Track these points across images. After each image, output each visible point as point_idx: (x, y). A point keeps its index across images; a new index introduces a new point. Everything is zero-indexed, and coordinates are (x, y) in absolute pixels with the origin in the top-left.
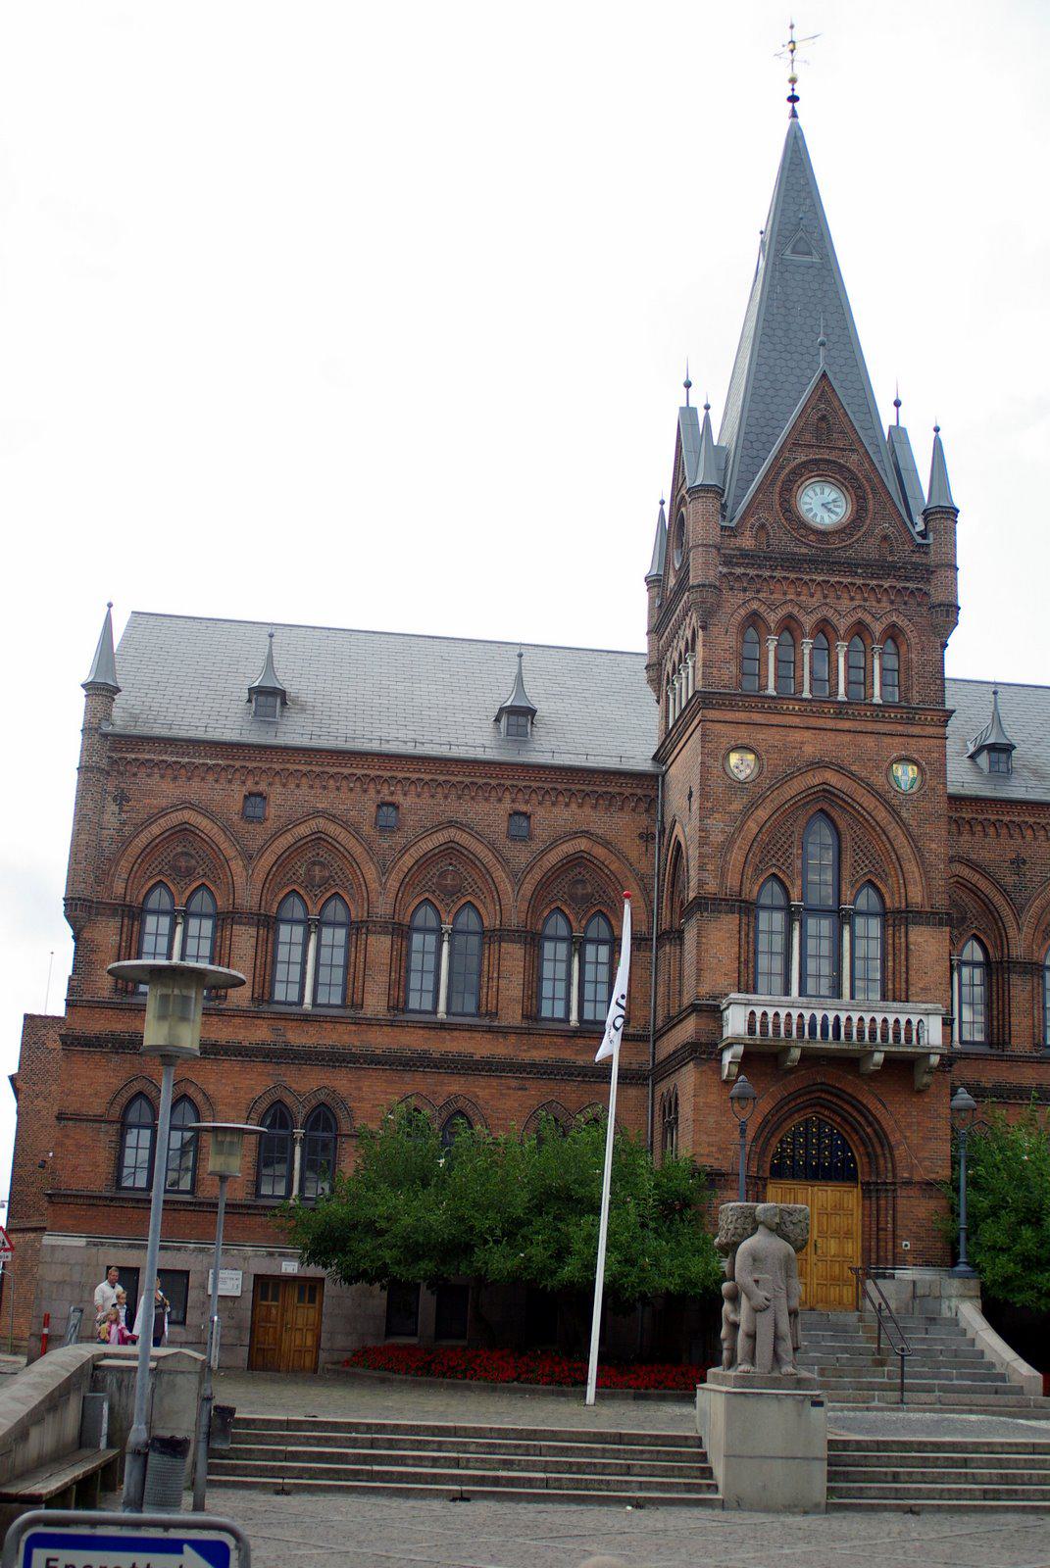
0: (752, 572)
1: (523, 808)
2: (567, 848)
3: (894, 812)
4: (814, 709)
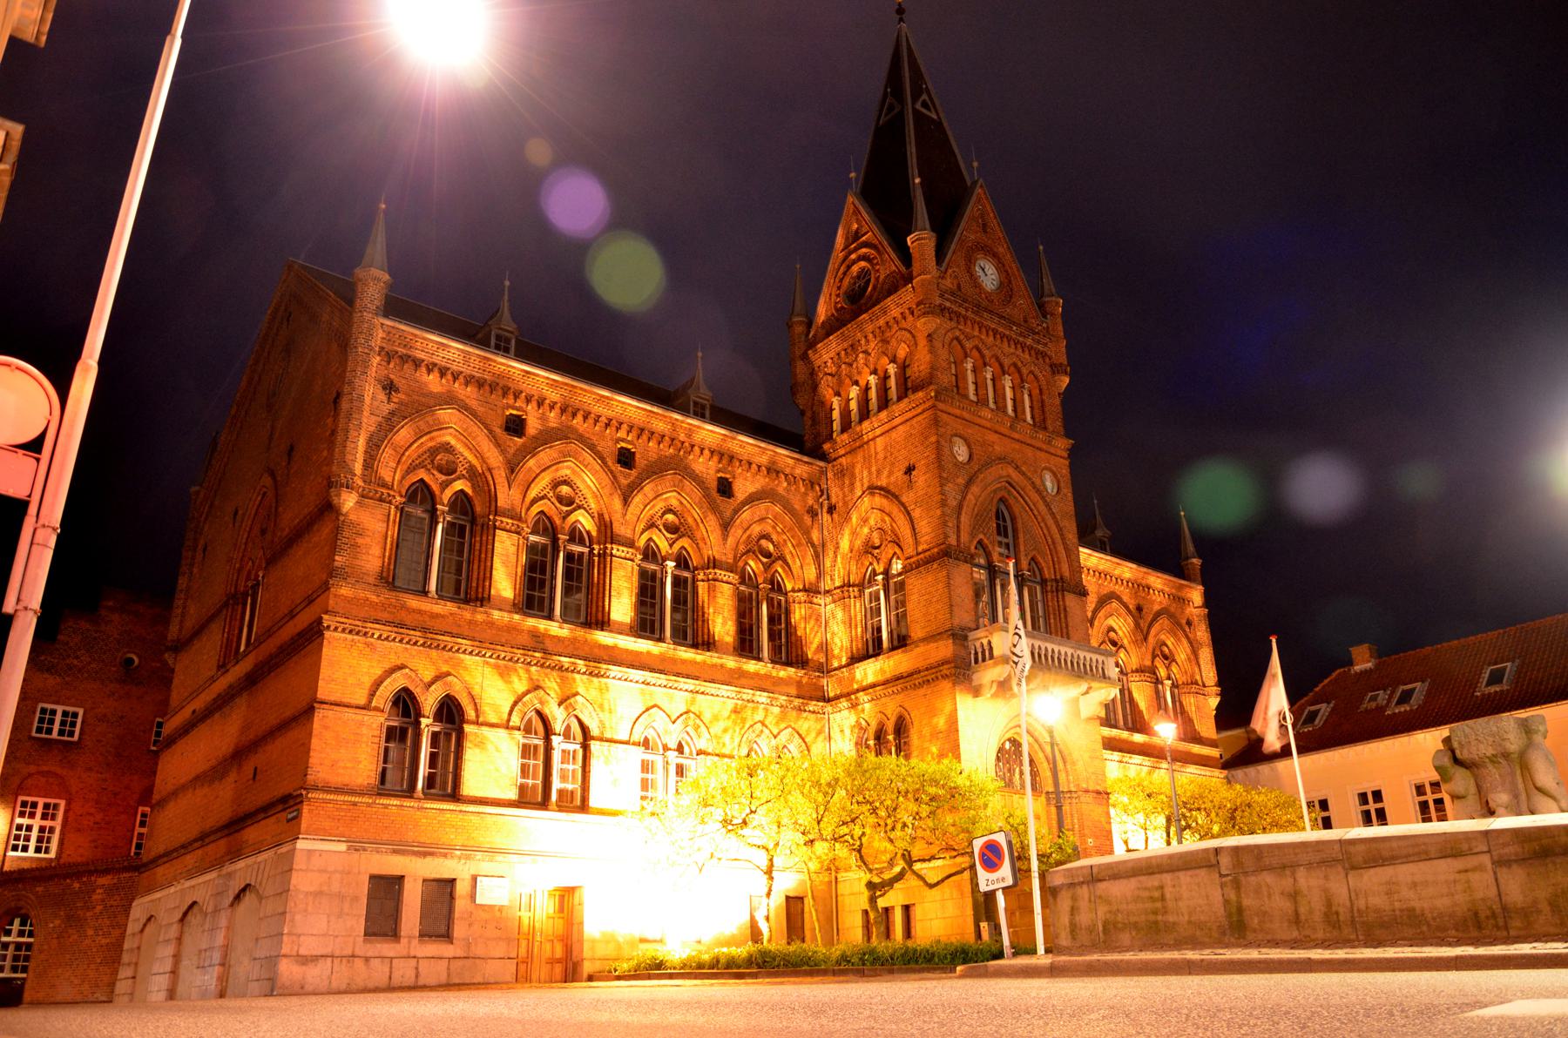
3: (1048, 505)
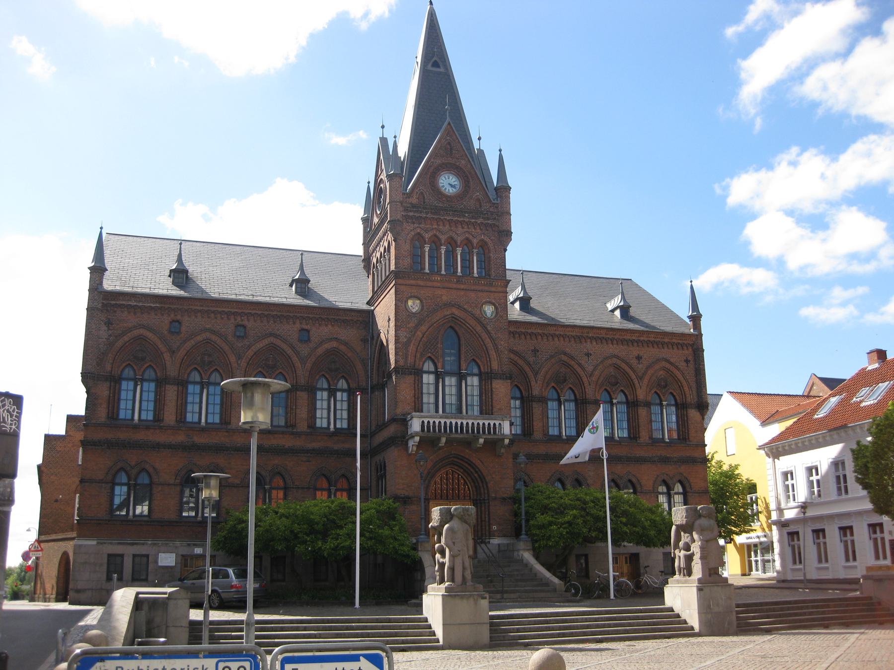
0: (417, 215)
2: (327, 346)
4: (447, 279)
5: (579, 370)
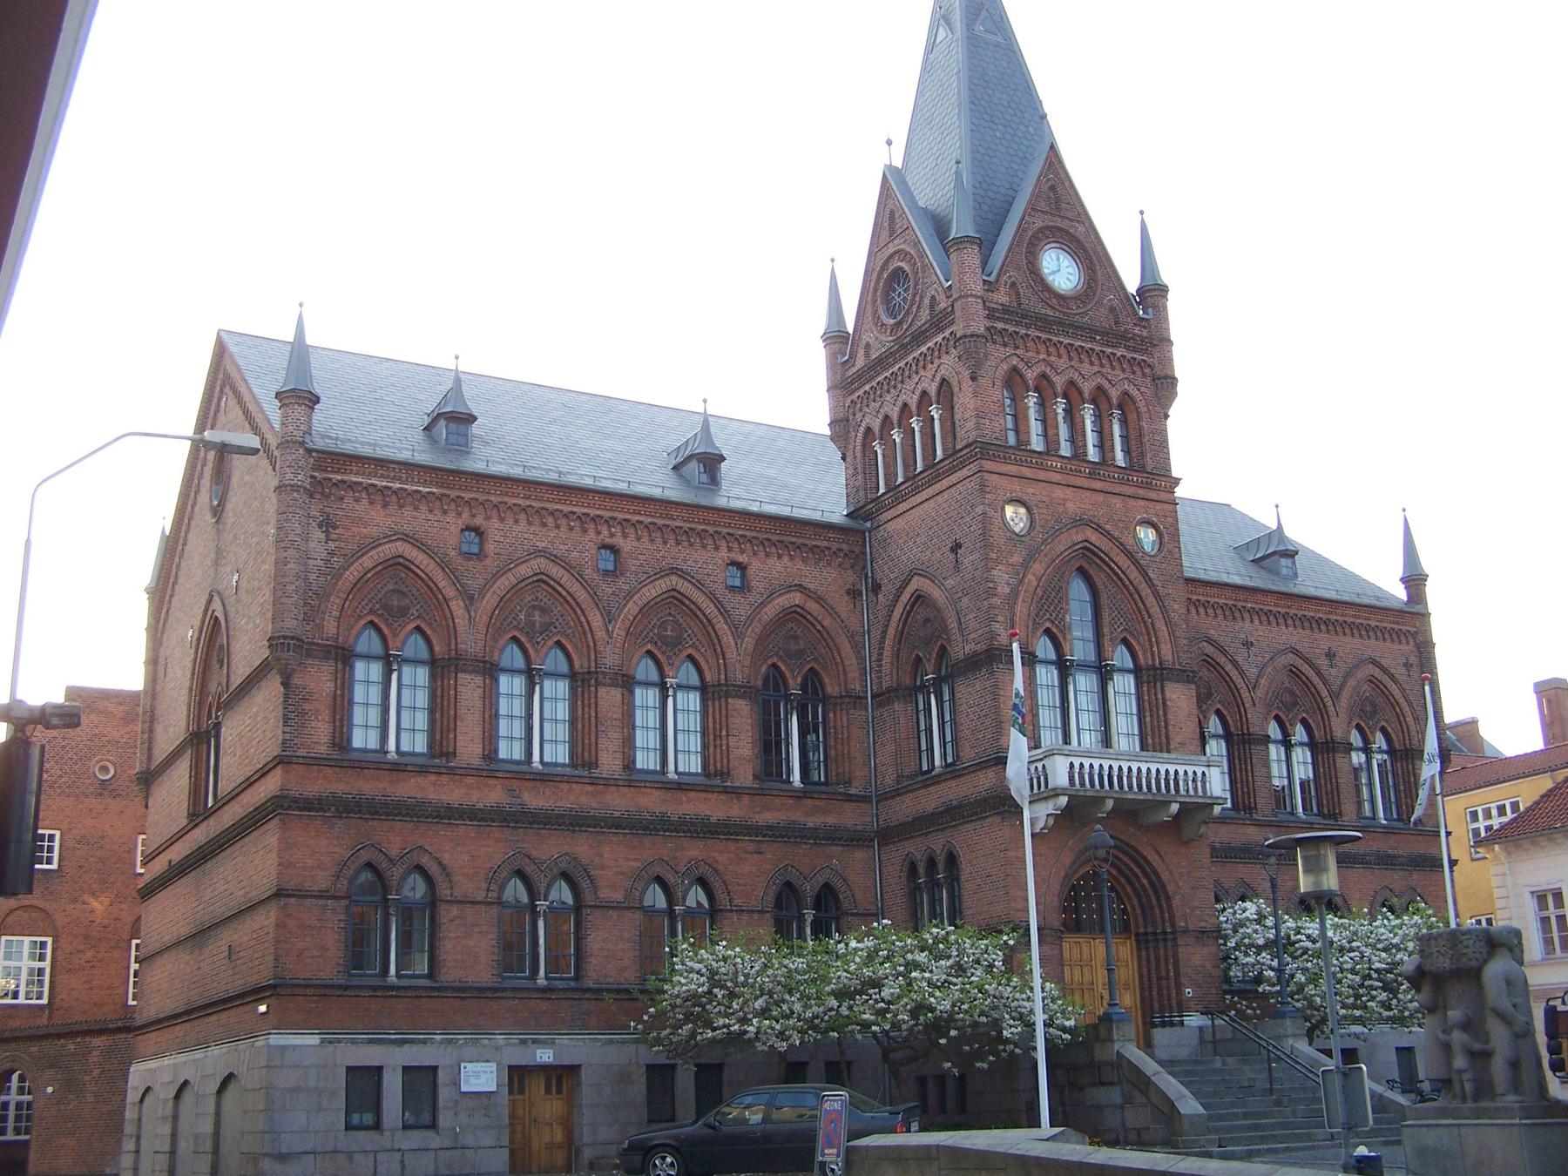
1: (741, 559)
3: (1143, 572)
5: (1234, 674)
